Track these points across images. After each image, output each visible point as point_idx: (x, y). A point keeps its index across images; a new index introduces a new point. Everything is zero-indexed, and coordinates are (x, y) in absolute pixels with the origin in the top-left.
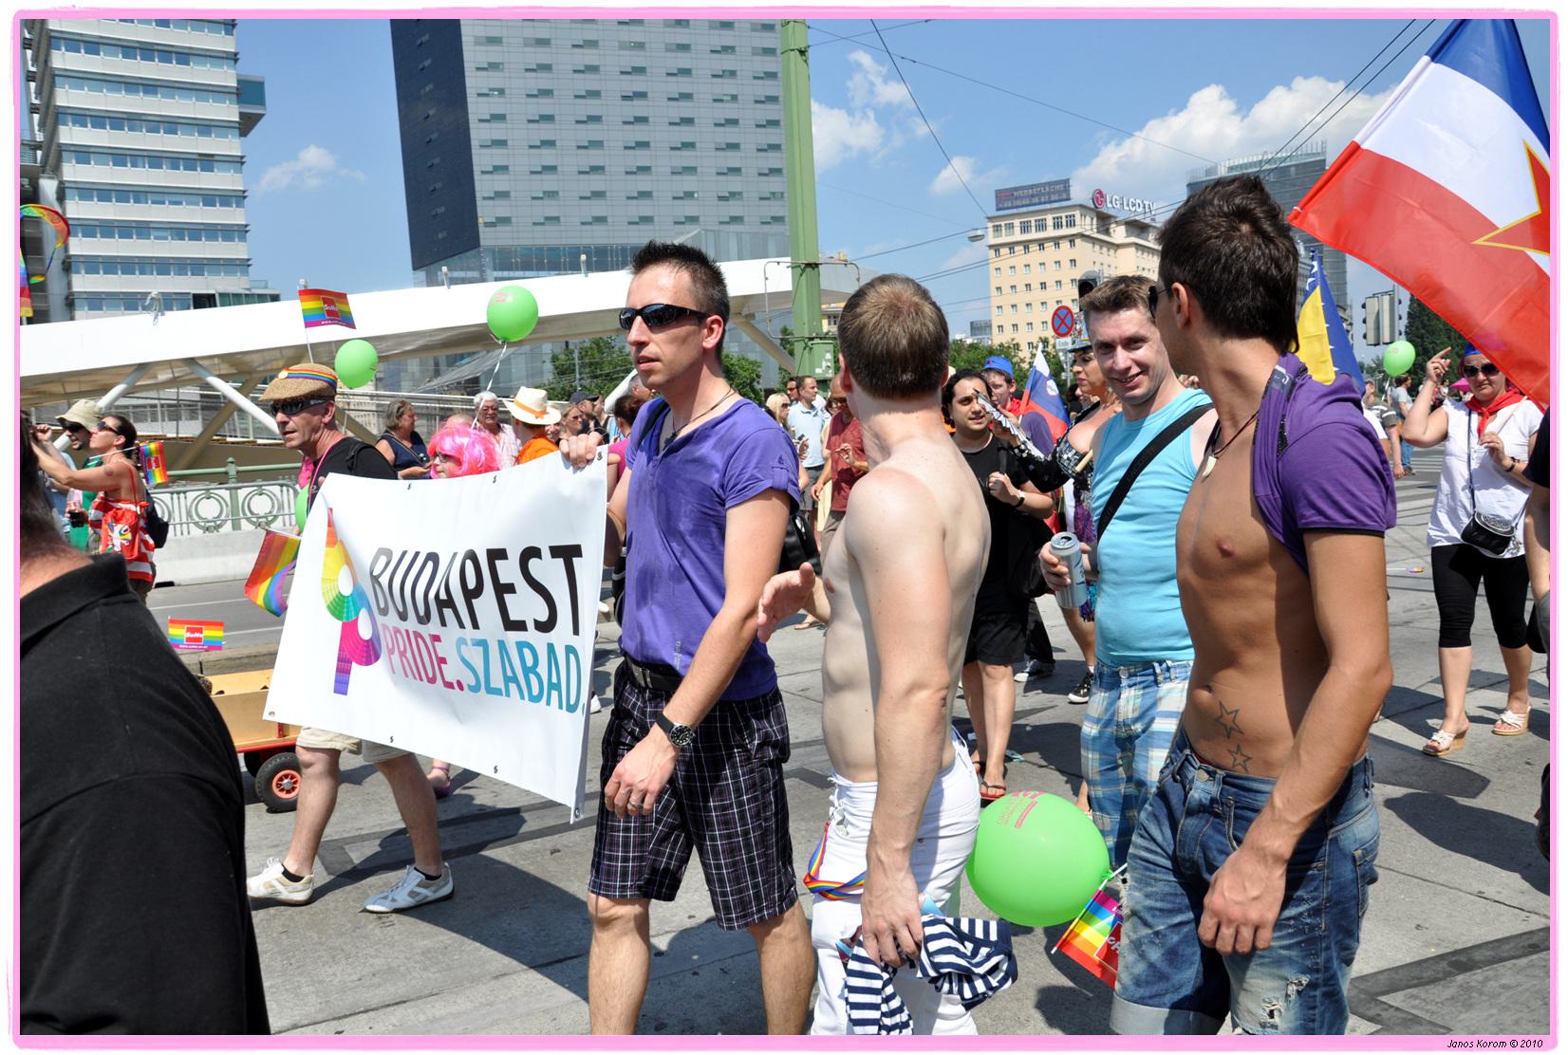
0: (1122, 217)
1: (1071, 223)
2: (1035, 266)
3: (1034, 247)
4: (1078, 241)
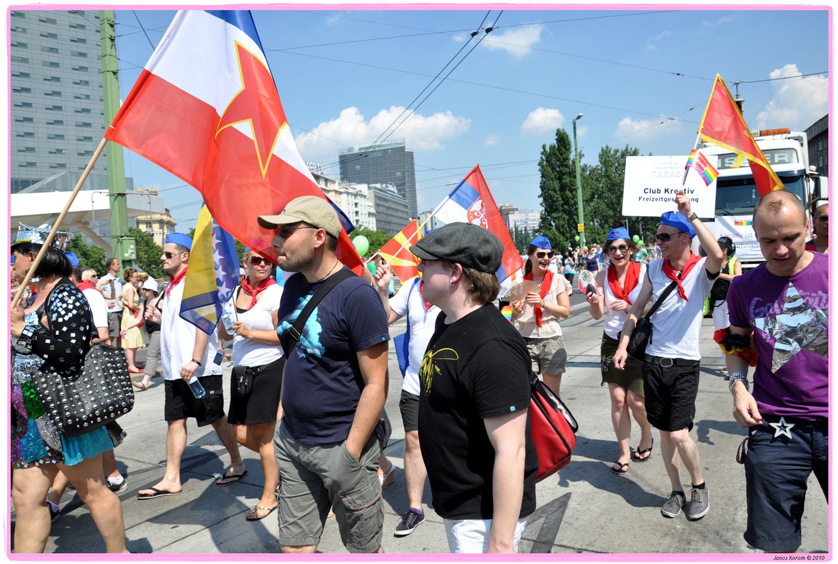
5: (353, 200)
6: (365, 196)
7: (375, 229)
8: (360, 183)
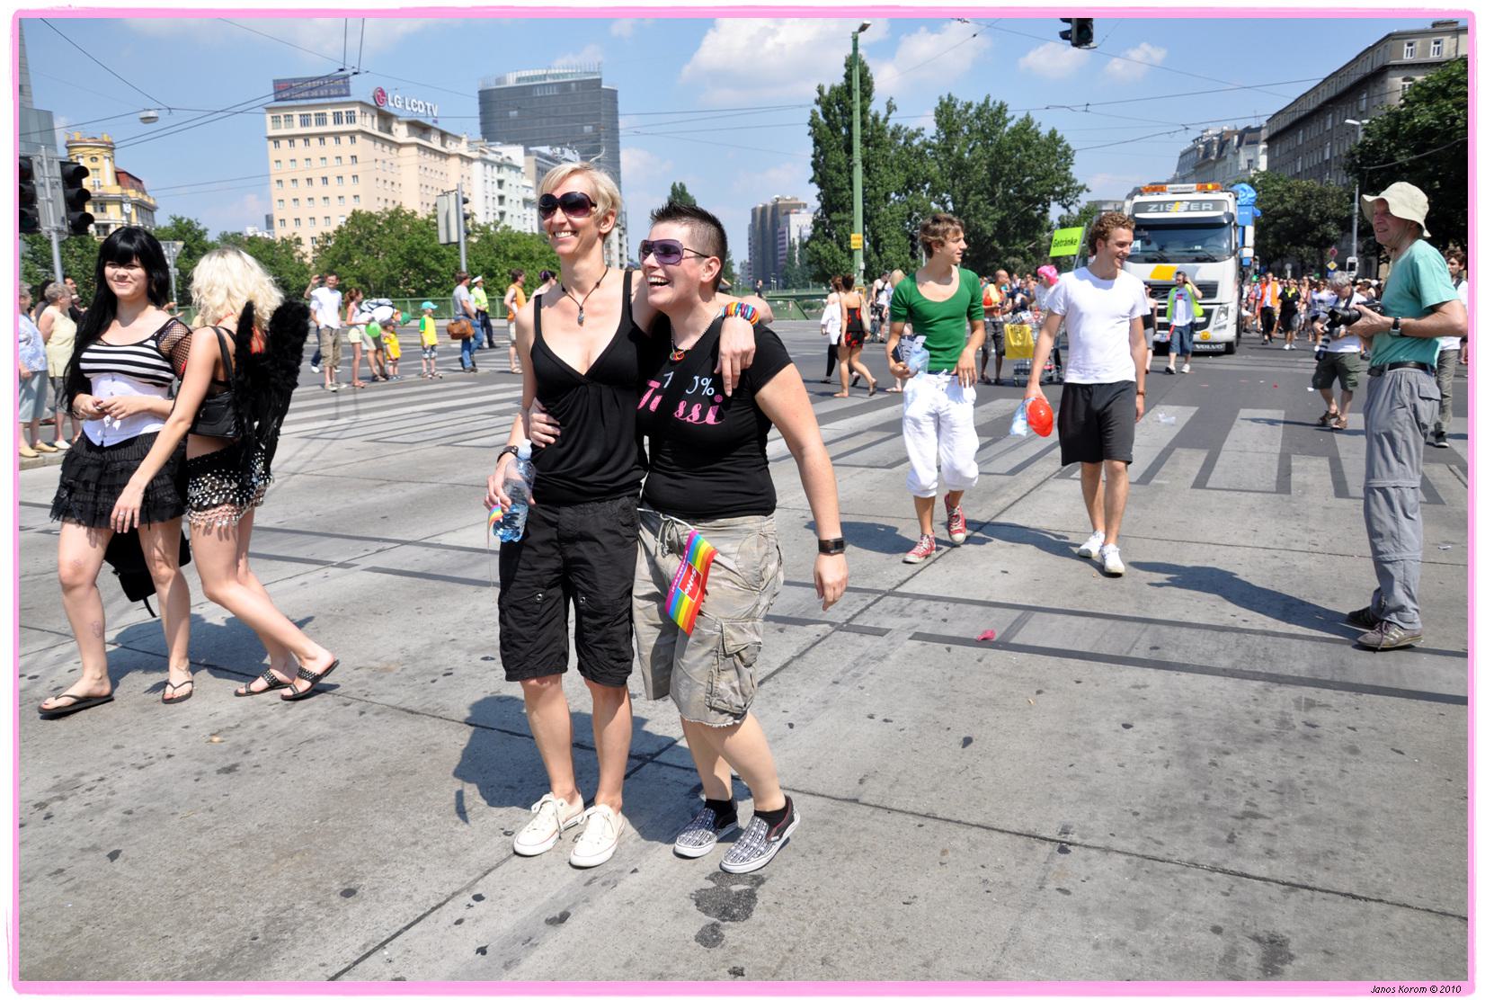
0: (406, 116)
1: (351, 119)
2: (316, 162)
3: (314, 141)
4: (358, 137)
5: (496, 175)
6: (517, 169)
7: (536, 231)
8: (511, 142)
